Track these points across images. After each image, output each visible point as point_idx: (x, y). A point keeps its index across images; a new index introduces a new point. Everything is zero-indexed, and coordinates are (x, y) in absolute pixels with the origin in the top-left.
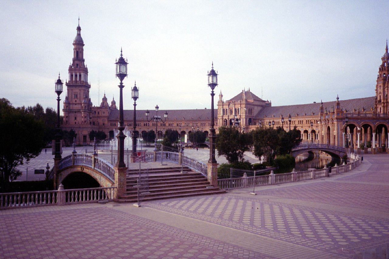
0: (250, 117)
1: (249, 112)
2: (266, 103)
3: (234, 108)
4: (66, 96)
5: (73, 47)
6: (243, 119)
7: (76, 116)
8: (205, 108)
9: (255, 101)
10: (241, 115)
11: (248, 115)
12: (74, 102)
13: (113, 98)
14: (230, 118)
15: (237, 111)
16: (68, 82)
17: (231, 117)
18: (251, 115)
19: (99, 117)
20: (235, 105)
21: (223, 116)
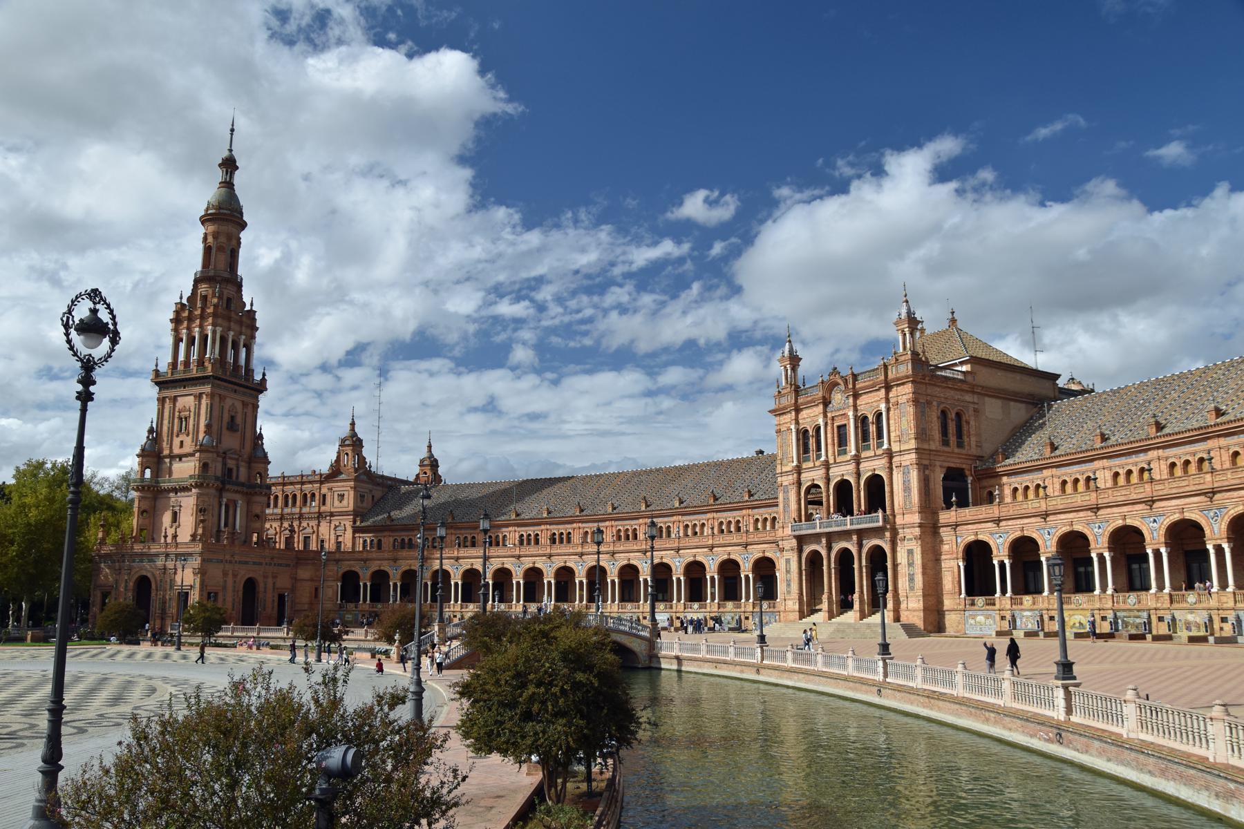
0: (955, 463)
1: (944, 432)
2: (1061, 383)
3: (851, 414)
4: (152, 427)
5: (201, 230)
6: (906, 474)
7: (177, 509)
8: (758, 449)
9: (978, 367)
10: (895, 448)
11: (935, 445)
12: (177, 451)
13: (430, 447)
14: (837, 473)
15: (872, 429)
16: (164, 367)
17: (843, 471)
18: (956, 450)
19: (320, 516)
20: (856, 396)
21: (799, 470)
